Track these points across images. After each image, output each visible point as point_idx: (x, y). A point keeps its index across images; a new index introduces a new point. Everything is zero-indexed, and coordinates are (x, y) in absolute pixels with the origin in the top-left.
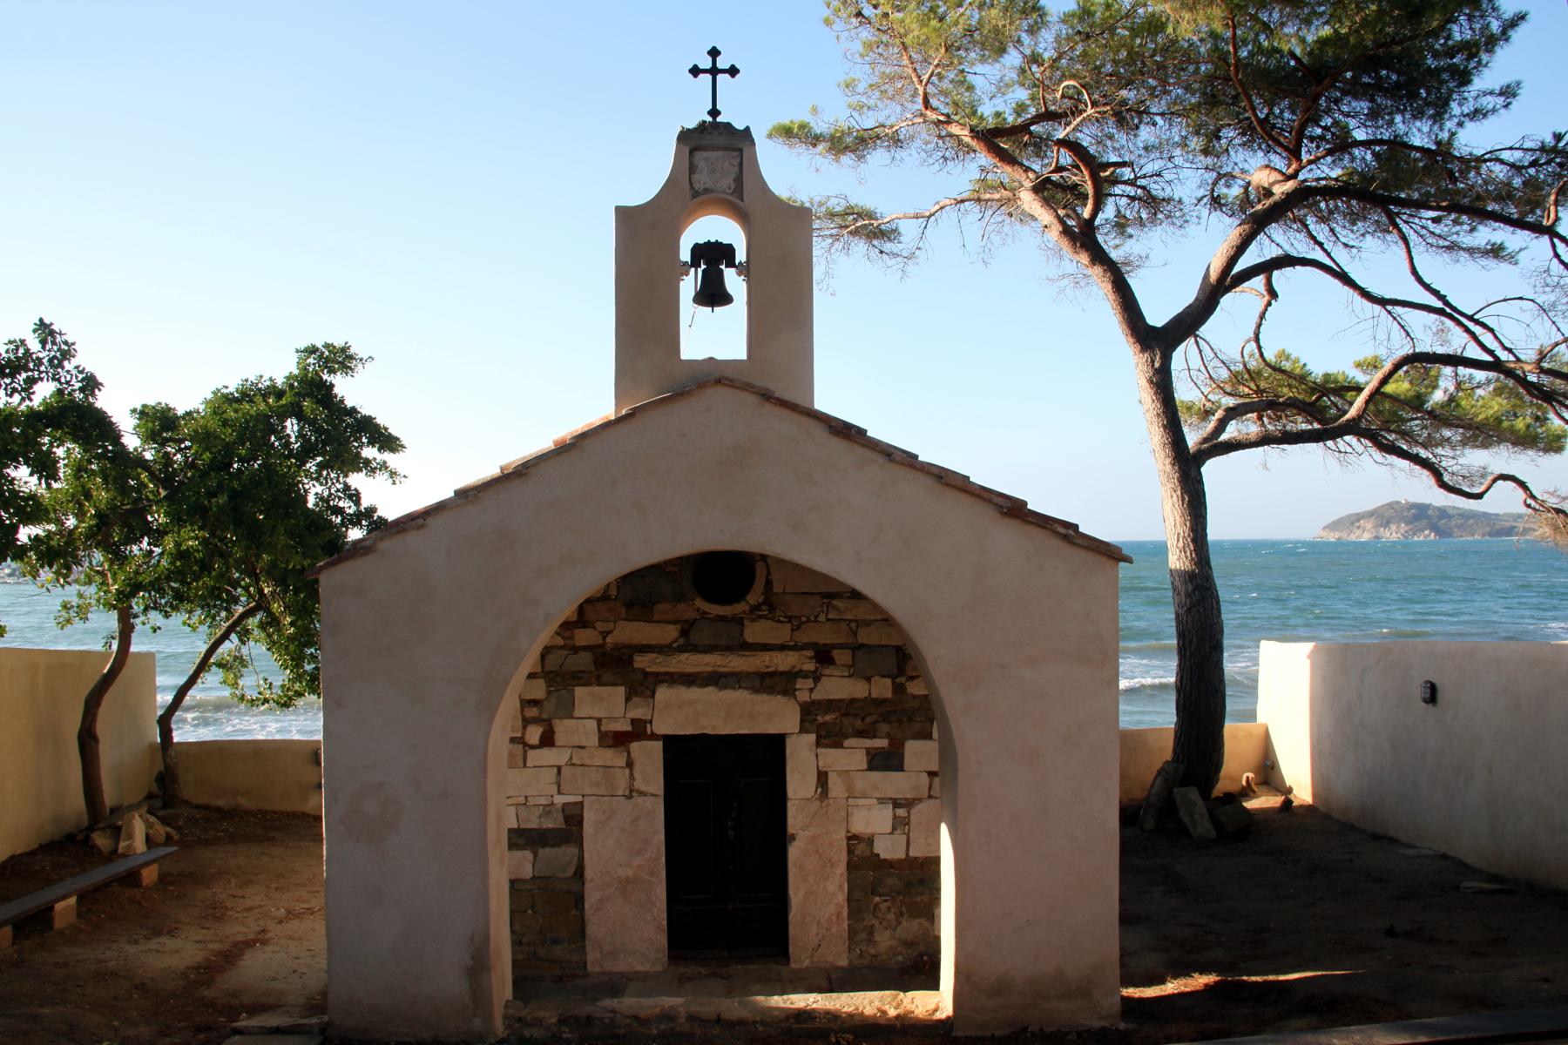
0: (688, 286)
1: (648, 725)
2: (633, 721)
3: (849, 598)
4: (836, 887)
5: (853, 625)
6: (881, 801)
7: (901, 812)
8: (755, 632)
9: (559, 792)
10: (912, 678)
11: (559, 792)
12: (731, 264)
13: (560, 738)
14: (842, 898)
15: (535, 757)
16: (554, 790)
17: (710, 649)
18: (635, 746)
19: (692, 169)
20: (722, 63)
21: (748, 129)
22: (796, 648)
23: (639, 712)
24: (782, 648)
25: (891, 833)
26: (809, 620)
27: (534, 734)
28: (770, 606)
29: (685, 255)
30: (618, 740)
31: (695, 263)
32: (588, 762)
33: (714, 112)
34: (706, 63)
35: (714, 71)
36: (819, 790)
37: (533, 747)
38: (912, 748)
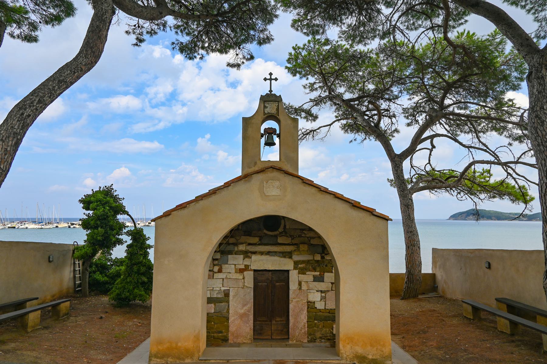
0: (263, 141)
1: (249, 267)
2: (245, 265)
3: (308, 230)
4: (304, 317)
5: (309, 238)
6: (317, 291)
7: (323, 295)
8: (280, 240)
9: (223, 286)
10: (326, 254)
11: (223, 286)
12: (275, 134)
13: (224, 270)
14: (305, 321)
15: (216, 275)
16: (221, 285)
18: (245, 273)
19: (265, 107)
20: (273, 77)
21: (280, 95)
22: (293, 245)
25: (320, 301)
26: (296, 237)
27: (216, 269)
28: (285, 233)
29: (262, 132)
30: (241, 271)
31: (265, 134)
32: (231, 277)
34: (268, 77)
35: (271, 79)
36: (299, 287)
37: (216, 273)
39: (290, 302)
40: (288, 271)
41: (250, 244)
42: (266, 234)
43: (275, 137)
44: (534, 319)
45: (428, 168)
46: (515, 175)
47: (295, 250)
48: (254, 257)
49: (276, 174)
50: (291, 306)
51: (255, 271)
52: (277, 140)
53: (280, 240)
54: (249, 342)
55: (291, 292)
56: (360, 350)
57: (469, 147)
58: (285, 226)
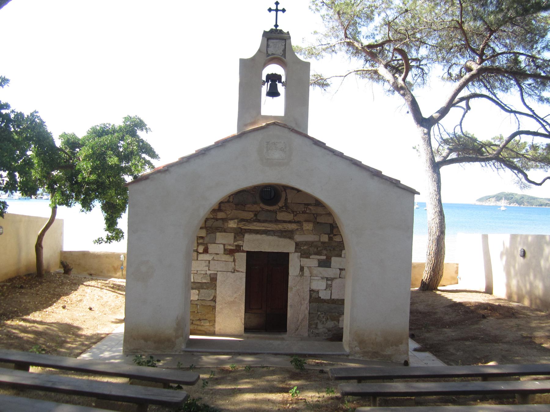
0: (265, 89)
1: (242, 248)
2: (236, 246)
3: (314, 206)
5: (315, 215)
6: (322, 278)
7: (329, 282)
8: (281, 216)
9: (209, 270)
10: (335, 235)
11: (209, 270)
12: (280, 82)
13: (210, 251)
14: (307, 312)
15: (201, 257)
16: (207, 268)
17: (265, 221)
18: (237, 255)
19: (268, 46)
20: (280, 7)
21: (288, 32)
22: (295, 222)
23: (240, 243)
24: (290, 222)
25: (325, 290)
26: (300, 213)
27: (201, 249)
28: (286, 208)
29: (264, 78)
31: (267, 81)
32: (219, 259)
33: (276, 26)
34: (274, 7)
35: (277, 10)
36: (301, 273)
37: (200, 253)
38: (334, 260)
40: (287, 255)
41: (242, 220)
47: (297, 229)
50: (290, 295)
51: (248, 252)
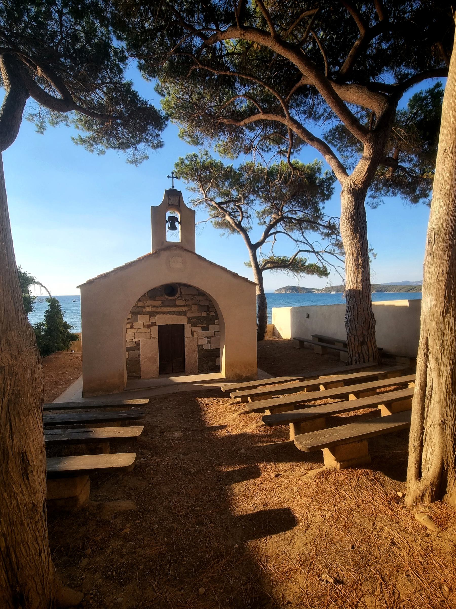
0: (168, 225)
4: (195, 356)
6: (204, 337)
7: (209, 339)
8: (178, 303)
14: (197, 358)
15: (128, 331)
17: (168, 306)
18: (152, 328)
19: (169, 199)
23: (153, 320)
24: (184, 306)
29: (167, 219)
30: (148, 326)
33: (173, 187)
38: (211, 326)
39: (185, 346)
40: (183, 325)
41: (155, 306)
42: (167, 299)
43: (176, 224)
44: (334, 344)
45: (271, 255)
46: (323, 261)
47: (188, 310)
48: (158, 316)
49: (178, 252)
50: (186, 349)
51: (159, 326)
52: (178, 226)
53: (178, 303)
54: (157, 376)
55: (186, 339)
56: (238, 372)
57: (296, 241)
58: (181, 292)
